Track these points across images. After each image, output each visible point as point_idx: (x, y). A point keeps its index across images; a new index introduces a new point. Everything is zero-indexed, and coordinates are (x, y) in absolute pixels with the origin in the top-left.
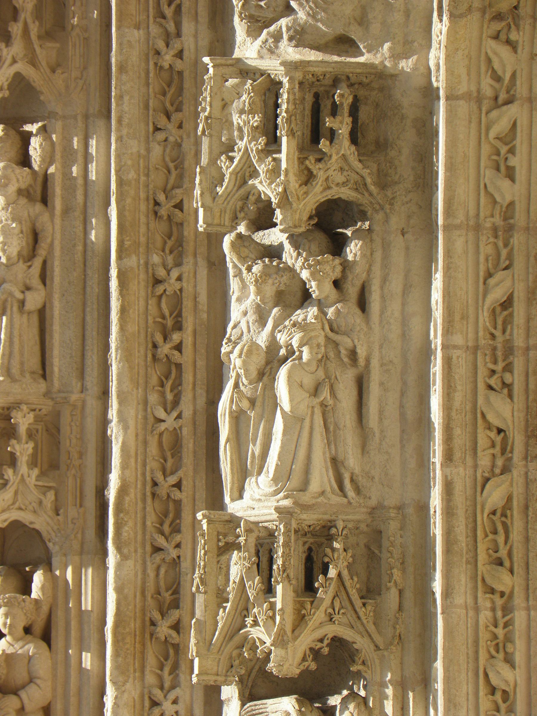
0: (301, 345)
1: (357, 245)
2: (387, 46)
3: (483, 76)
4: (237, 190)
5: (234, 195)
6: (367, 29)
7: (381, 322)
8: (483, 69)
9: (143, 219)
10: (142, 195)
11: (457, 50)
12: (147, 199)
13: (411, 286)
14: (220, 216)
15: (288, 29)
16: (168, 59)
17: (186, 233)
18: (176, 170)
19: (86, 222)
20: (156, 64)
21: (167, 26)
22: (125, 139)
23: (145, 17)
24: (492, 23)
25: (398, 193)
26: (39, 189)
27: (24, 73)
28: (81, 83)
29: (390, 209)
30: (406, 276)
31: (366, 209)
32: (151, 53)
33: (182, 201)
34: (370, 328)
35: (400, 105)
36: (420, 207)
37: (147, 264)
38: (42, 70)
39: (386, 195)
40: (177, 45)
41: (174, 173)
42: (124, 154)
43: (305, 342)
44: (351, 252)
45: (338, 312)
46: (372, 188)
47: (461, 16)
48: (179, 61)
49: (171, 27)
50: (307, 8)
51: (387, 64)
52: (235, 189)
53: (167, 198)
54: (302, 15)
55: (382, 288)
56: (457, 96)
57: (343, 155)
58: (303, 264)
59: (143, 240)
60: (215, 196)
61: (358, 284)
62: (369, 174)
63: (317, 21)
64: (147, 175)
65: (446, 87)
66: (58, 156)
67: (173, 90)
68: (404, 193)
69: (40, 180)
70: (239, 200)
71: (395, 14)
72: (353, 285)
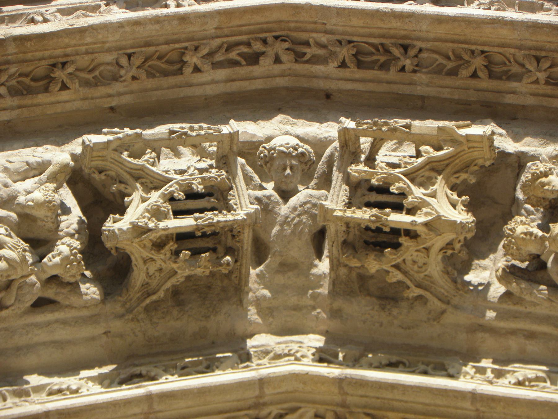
0: (7, 260)
1: (94, 294)
2: (267, 293)
3: (279, 406)
4: (126, 171)
5: (122, 169)
6: (278, 272)
7: (28, 325)
8: (285, 406)
9: (47, 53)
10: (68, 50)
11: (305, 383)
12: (66, 55)
13: (62, 348)
14: (99, 156)
15: (269, 197)
16: (193, 59)
17: (40, 96)
18: (93, 78)
20: (186, 48)
21: (220, 54)
22: (121, 30)
23: (226, 32)
24: (332, 413)
25: (142, 324)
29: (128, 319)
30: (69, 342)
31: (123, 295)
32: (195, 43)
33: (68, 88)
34: (21, 316)
35: (217, 312)
36: (130, 345)
37: (8, 62)
39: (140, 314)
40: (206, 67)
41: (89, 76)
42: (108, 31)
43: (11, 263)
44: (88, 289)
45: (34, 285)
46: (148, 301)
47: (341, 388)
48: (191, 69)
49: (219, 57)
50: (292, 216)
51: (251, 295)
52: (128, 170)
53: (70, 74)
54: (284, 209)
55: (57, 321)
56: (263, 388)
57: (177, 272)
58: (75, 248)
59: (29, 56)
60: (118, 150)
61: (59, 298)
62: (160, 296)
63: (282, 225)
64: (87, 53)
65: (270, 377)
67: (164, 66)
68: (143, 329)
70: (116, 173)
71: (295, 298)
72: (56, 294)
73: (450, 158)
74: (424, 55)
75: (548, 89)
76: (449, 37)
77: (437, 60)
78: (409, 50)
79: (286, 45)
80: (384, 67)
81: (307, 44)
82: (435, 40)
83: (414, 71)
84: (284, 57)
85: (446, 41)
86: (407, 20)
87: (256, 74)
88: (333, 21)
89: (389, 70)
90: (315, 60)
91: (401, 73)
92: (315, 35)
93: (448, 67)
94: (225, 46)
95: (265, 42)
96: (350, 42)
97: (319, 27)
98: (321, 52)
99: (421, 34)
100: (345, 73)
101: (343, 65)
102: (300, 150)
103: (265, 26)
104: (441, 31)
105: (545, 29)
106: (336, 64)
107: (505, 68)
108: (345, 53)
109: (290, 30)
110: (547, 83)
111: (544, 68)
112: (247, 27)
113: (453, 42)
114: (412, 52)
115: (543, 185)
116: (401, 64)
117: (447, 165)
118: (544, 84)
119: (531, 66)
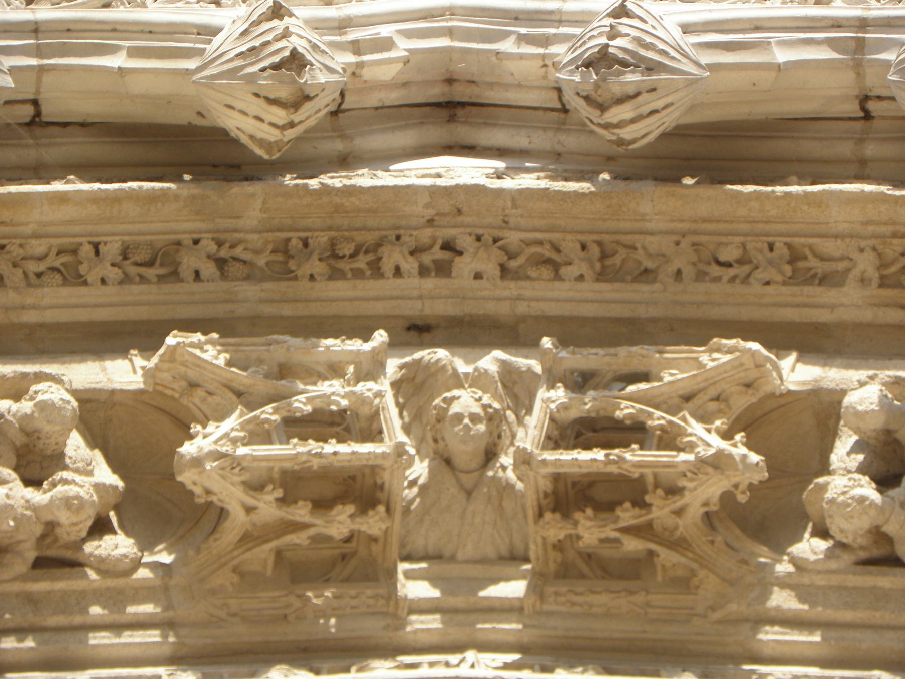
19: (20, 632)
26: (52, 553)
27: (227, 524)
28: (223, 614)
38: (236, 553)
66: (111, 583)
69: (68, 554)
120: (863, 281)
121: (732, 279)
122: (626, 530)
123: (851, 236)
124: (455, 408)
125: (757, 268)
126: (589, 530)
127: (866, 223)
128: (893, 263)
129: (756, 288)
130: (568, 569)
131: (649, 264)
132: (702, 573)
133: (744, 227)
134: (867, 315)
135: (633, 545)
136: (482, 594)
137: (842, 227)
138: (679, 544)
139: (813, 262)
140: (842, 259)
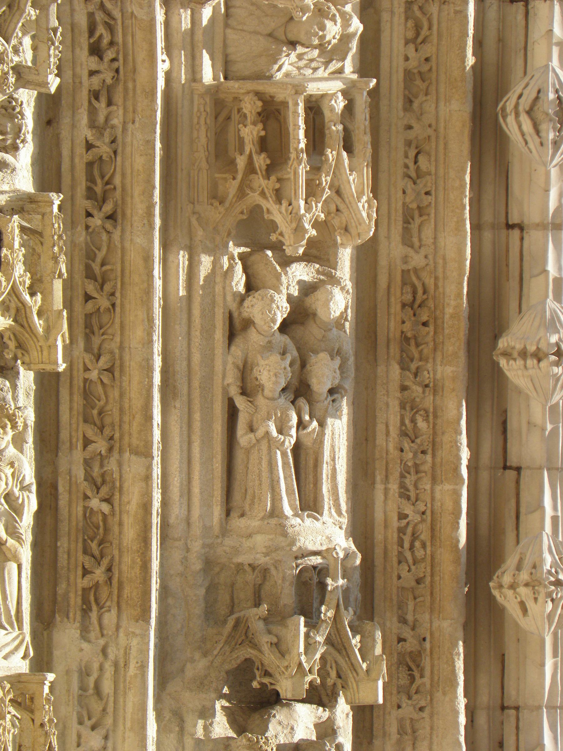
21: (102, 16)
23: (127, 21)
49: (99, 16)
73: (31, 330)
74: (104, 236)
75: (79, 383)
76: (127, 264)
77: (99, 249)
78: (111, 221)
79: (109, 81)
80: (90, 194)
81: (110, 103)
82: (123, 249)
83: (87, 227)
84: (96, 80)
85: (123, 262)
86: (146, 222)
87: (78, 51)
88: (139, 135)
89: (88, 198)
90: (92, 112)
91: (84, 212)
92: (121, 112)
93: (93, 265)
94: (112, 23)
95: (114, 60)
96: (115, 152)
97: (130, 116)
98: (101, 118)
99: (128, 234)
100: (80, 149)
101: (89, 146)
102: (21, 145)
103: (130, 58)
104: (134, 257)
105: (147, 380)
106: (90, 138)
107: (96, 329)
108: (104, 149)
109: (125, 82)
110: (85, 380)
111: (102, 377)
112: (131, 41)
113: (123, 271)
114: (108, 226)
115: (4, 427)
116: (95, 212)
117: (22, 326)
118: (84, 378)
119: (103, 362)
120: (405, 259)
121: (406, 166)
122: (250, 157)
123: (436, 248)
124: (329, 24)
125: (415, 183)
126: (250, 133)
127: (444, 259)
128: (418, 278)
129: (401, 183)
130: (221, 107)
131: (416, 105)
132: (221, 209)
133: (441, 172)
134: (383, 262)
135: (241, 162)
136: (204, 51)
137: (441, 242)
138: (241, 194)
139: (418, 221)
140: (420, 240)
